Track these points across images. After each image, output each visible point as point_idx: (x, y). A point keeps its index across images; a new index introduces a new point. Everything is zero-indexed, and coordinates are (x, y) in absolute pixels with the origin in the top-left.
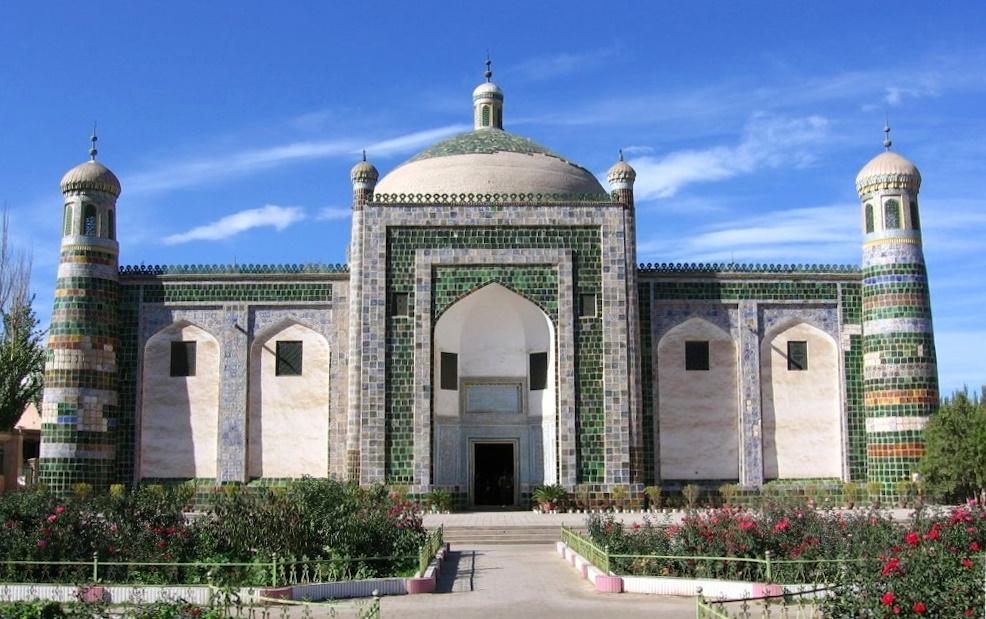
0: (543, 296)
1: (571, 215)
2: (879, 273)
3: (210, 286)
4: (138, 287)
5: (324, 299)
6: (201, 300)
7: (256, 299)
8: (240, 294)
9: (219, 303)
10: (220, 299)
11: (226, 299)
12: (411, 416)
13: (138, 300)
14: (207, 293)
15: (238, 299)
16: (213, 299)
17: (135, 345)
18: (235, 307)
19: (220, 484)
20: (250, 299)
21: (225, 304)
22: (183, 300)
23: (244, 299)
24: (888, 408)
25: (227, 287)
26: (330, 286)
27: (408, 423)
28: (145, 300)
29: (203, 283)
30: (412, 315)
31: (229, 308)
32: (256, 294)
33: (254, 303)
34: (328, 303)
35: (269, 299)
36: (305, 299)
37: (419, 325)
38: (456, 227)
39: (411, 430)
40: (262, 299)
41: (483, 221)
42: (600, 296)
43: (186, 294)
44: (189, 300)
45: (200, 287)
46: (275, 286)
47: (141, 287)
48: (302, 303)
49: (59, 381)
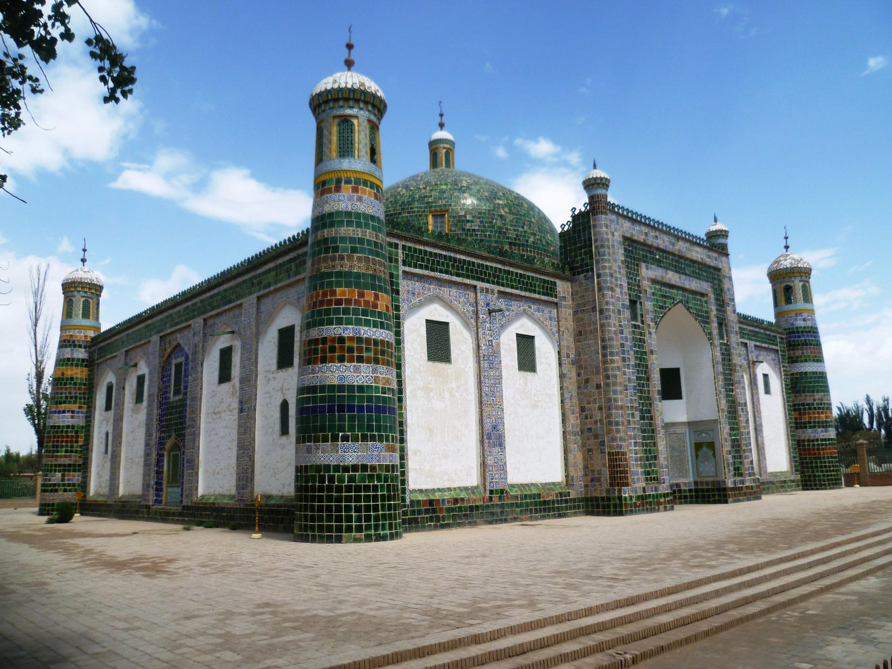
0: (704, 319)
1: (709, 256)
2: (802, 332)
3: (464, 260)
4: (396, 246)
5: (552, 296)
6: (458, 275)
7: (503, 285)
8: (489, 276)
9: (474, 283)
10: (474, 278)
11: (478, 279)
12: (651, 418)
13: (397, 261)
14: (462, 267)
15: (488, 282)
16: (468, 277)
17: (398, 317)
18: (487, 290)
19: (488, 495)
20: (498, 284)
21: (479, 284)
22: (441, 272)
23: (493, 283)
24: (819, 422)
25: (479, 265)
26: (555, 284)
27: (651, 425)
28: (405, 263)
29: (458, 256)
30: (643, 322)
31: (482, 290)
32: (502, 279)
33: (502, 289)
34: (555, 300)
35: (512, 287)
36: (539, 293)
37: (650, 333)
38: (658, 249)
39: (653, 431)
40: (508, 286)
41: (670, 248)
42: (726, 326)
43: (443, 264)
44: (447, 272)
45: (455, 260)
46: (517, 273)
47: (400, 247)
48: (537, 296)
49: (365, 355)
